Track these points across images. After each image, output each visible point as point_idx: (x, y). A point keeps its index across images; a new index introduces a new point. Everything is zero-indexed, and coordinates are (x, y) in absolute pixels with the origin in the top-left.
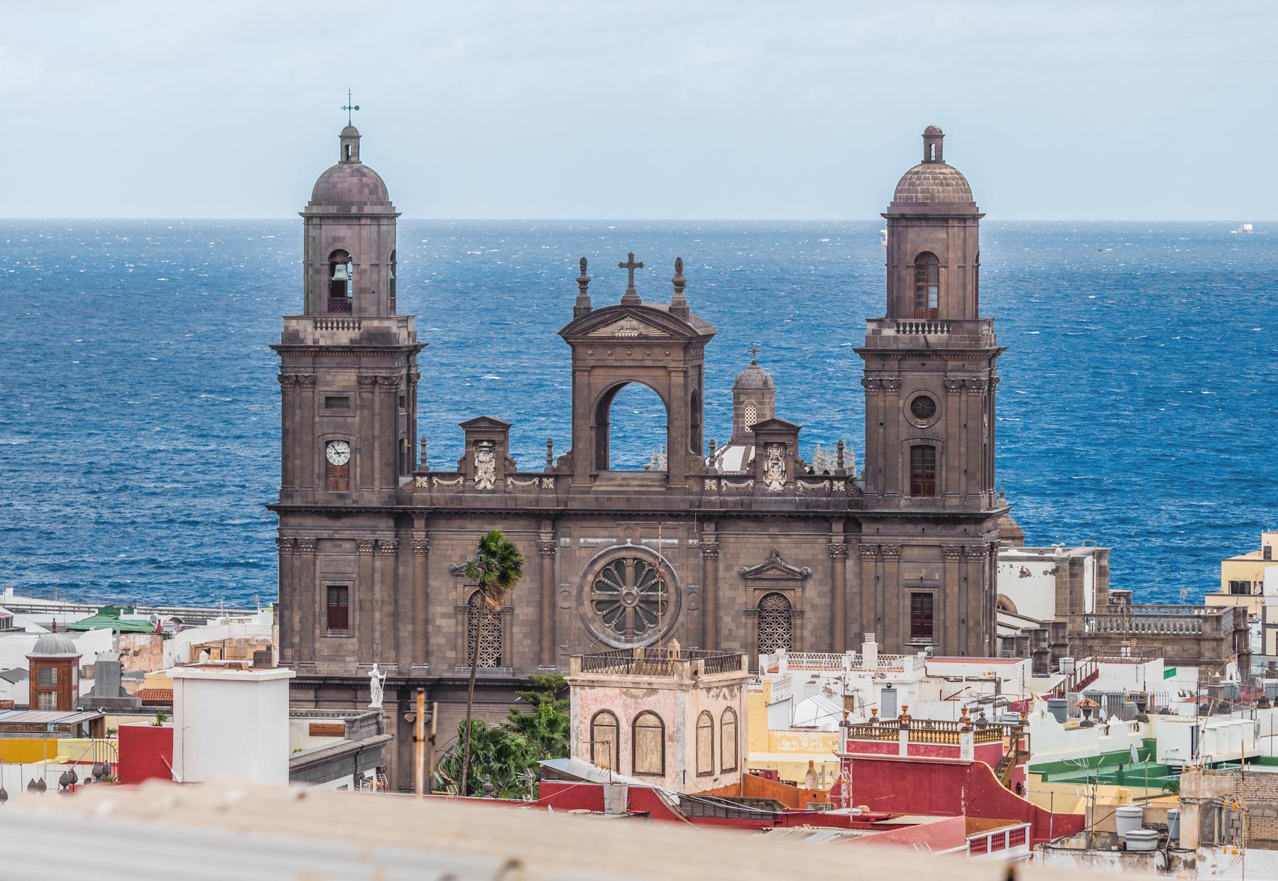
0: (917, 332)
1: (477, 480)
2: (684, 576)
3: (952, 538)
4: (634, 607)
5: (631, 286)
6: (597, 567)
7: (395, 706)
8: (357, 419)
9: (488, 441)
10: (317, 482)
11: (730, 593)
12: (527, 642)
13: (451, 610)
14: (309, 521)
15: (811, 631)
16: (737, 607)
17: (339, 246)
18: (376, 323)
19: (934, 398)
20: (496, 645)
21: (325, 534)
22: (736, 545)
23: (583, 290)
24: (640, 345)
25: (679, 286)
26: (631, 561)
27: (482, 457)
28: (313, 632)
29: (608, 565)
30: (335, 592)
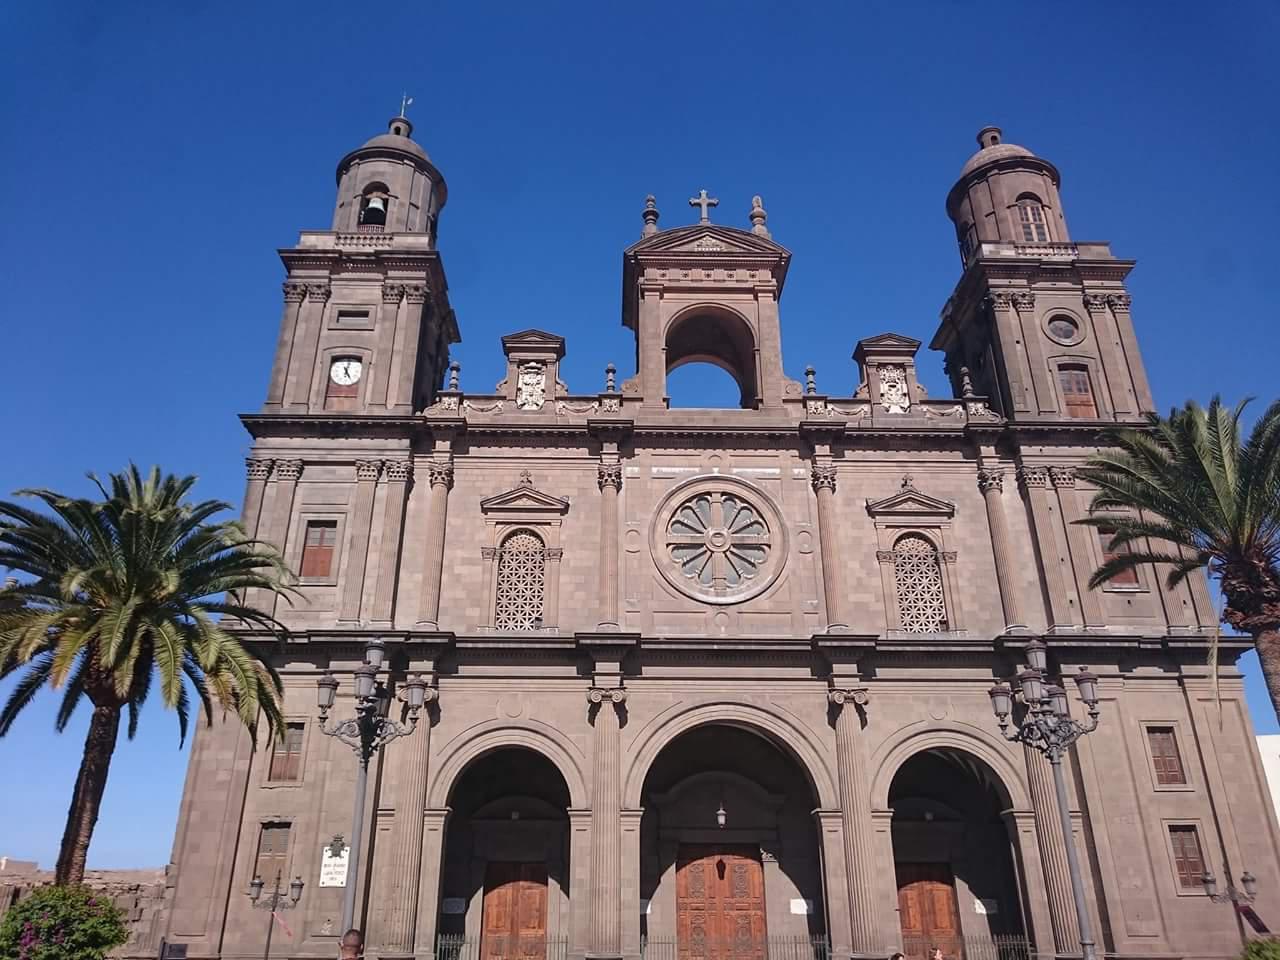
1: (519, 402)
4: (724, 552)
6: (676, 502)
9: (537, 362)
10: (313, 399)
12: (580, 595)
15: (969, 580)
26: (719, 495)
27: (527, 378)
29: (687, 501)
30: (316, 532)
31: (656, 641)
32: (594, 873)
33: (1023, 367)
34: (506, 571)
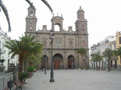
2: (63, 39)
3: (86, 36)
25: (62, 15)
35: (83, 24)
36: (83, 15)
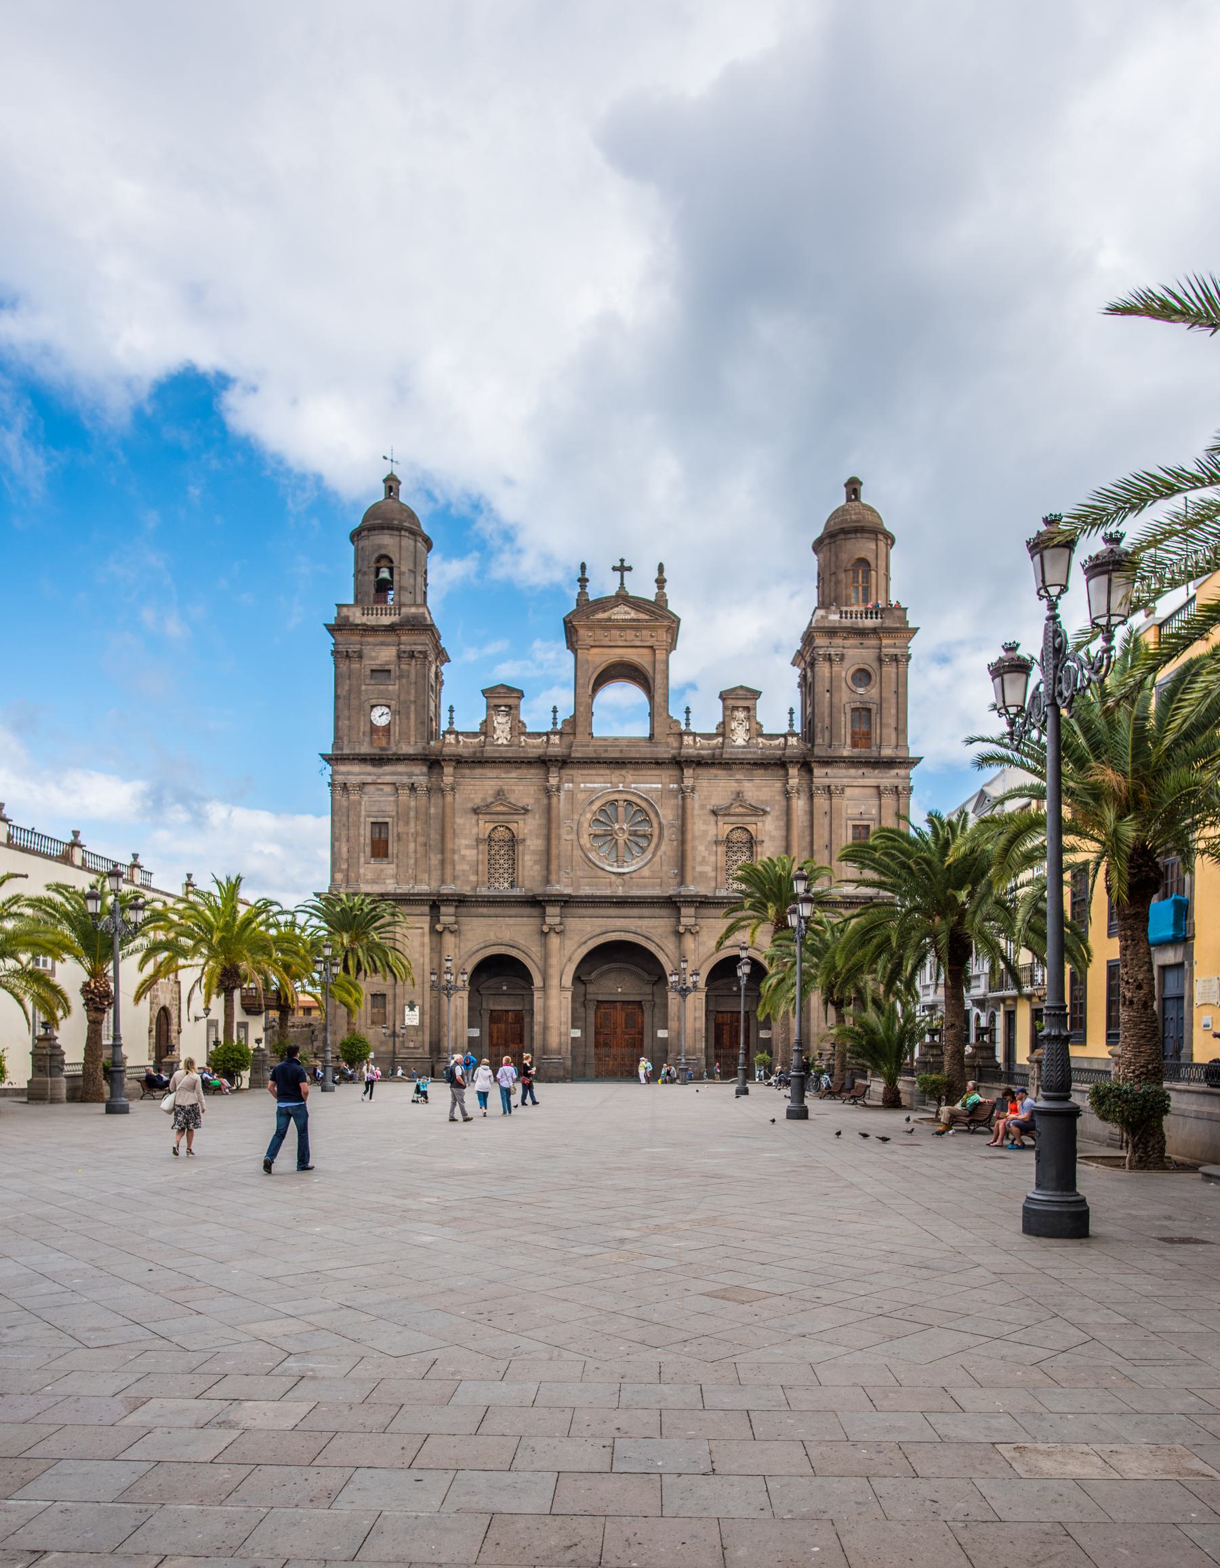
0: (856, 618)
2: (667, 814)
3: (887, 779)
5: (622, 584)
6: (595, 807)
7: (428, 919)
8: (397, 687)
9: (506, 706)
11: (704, 828)
13: (475, 843)
14: (356, 768)
16: (709, 838)
17: (383, 552)
18: (413, 610)
19: (870, 670)
20: (510, 871)
21: (369, 779)
22: (710, 789)
23: (583, 587)
24: (631, 628)
25: (661, 582)
28: (359, 859)
31: (581, 897)
32: (546, 1019)
33: (827, 711)
34: (493, 852)
35: (858, 654)
36: (867, 578)
